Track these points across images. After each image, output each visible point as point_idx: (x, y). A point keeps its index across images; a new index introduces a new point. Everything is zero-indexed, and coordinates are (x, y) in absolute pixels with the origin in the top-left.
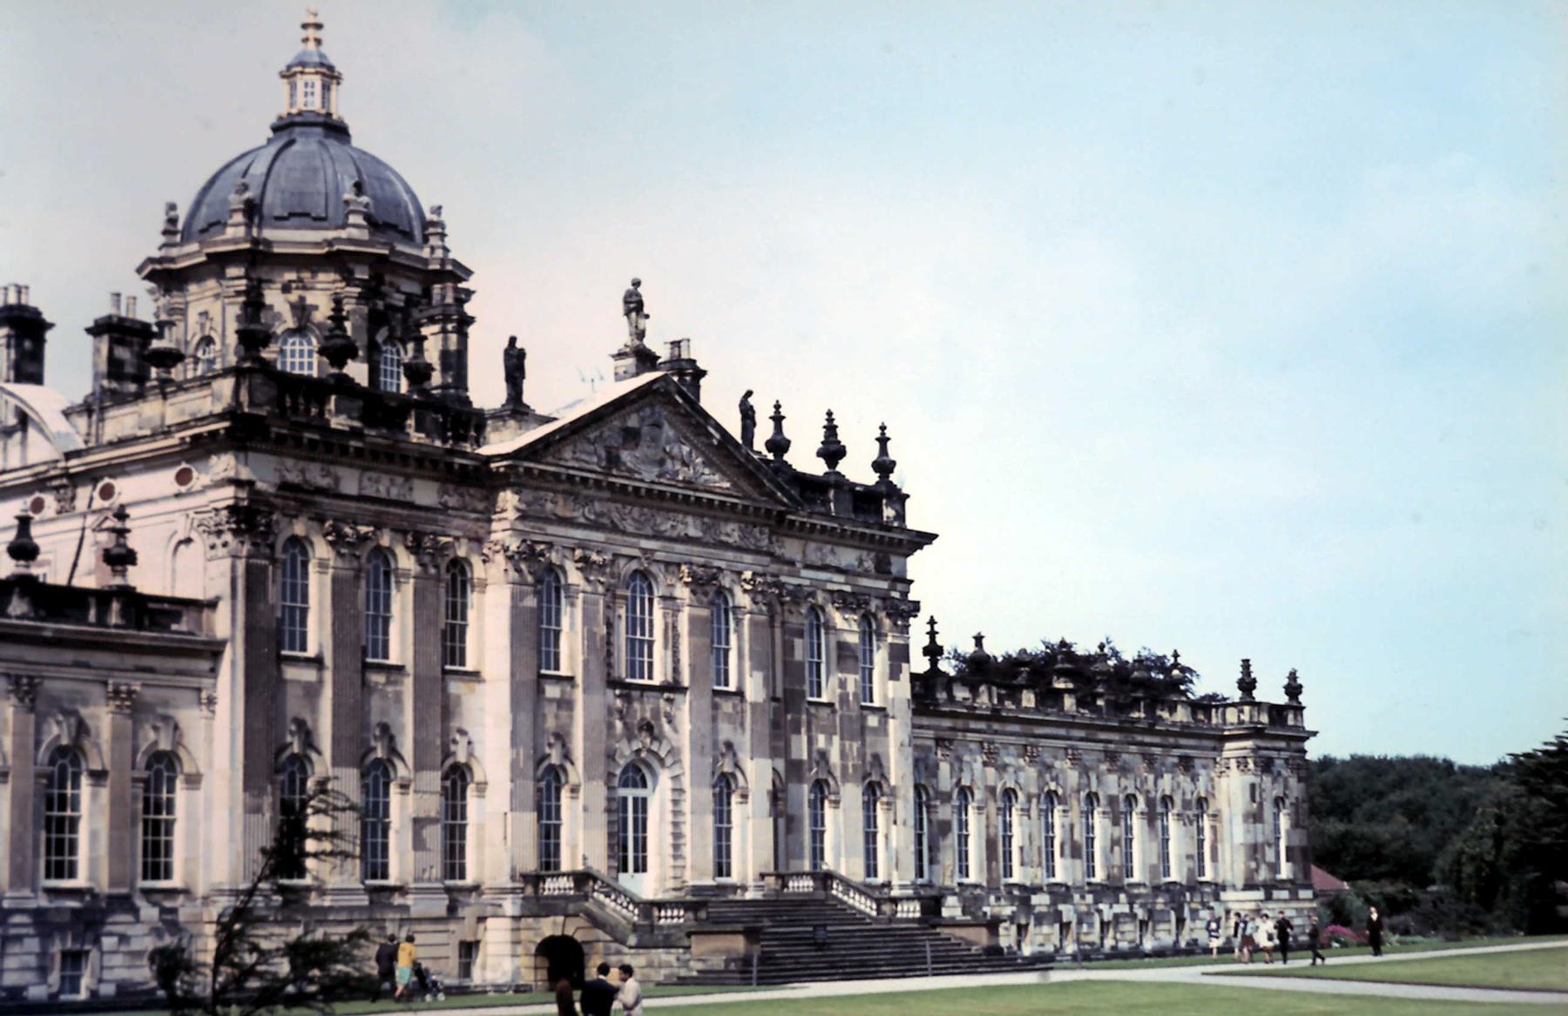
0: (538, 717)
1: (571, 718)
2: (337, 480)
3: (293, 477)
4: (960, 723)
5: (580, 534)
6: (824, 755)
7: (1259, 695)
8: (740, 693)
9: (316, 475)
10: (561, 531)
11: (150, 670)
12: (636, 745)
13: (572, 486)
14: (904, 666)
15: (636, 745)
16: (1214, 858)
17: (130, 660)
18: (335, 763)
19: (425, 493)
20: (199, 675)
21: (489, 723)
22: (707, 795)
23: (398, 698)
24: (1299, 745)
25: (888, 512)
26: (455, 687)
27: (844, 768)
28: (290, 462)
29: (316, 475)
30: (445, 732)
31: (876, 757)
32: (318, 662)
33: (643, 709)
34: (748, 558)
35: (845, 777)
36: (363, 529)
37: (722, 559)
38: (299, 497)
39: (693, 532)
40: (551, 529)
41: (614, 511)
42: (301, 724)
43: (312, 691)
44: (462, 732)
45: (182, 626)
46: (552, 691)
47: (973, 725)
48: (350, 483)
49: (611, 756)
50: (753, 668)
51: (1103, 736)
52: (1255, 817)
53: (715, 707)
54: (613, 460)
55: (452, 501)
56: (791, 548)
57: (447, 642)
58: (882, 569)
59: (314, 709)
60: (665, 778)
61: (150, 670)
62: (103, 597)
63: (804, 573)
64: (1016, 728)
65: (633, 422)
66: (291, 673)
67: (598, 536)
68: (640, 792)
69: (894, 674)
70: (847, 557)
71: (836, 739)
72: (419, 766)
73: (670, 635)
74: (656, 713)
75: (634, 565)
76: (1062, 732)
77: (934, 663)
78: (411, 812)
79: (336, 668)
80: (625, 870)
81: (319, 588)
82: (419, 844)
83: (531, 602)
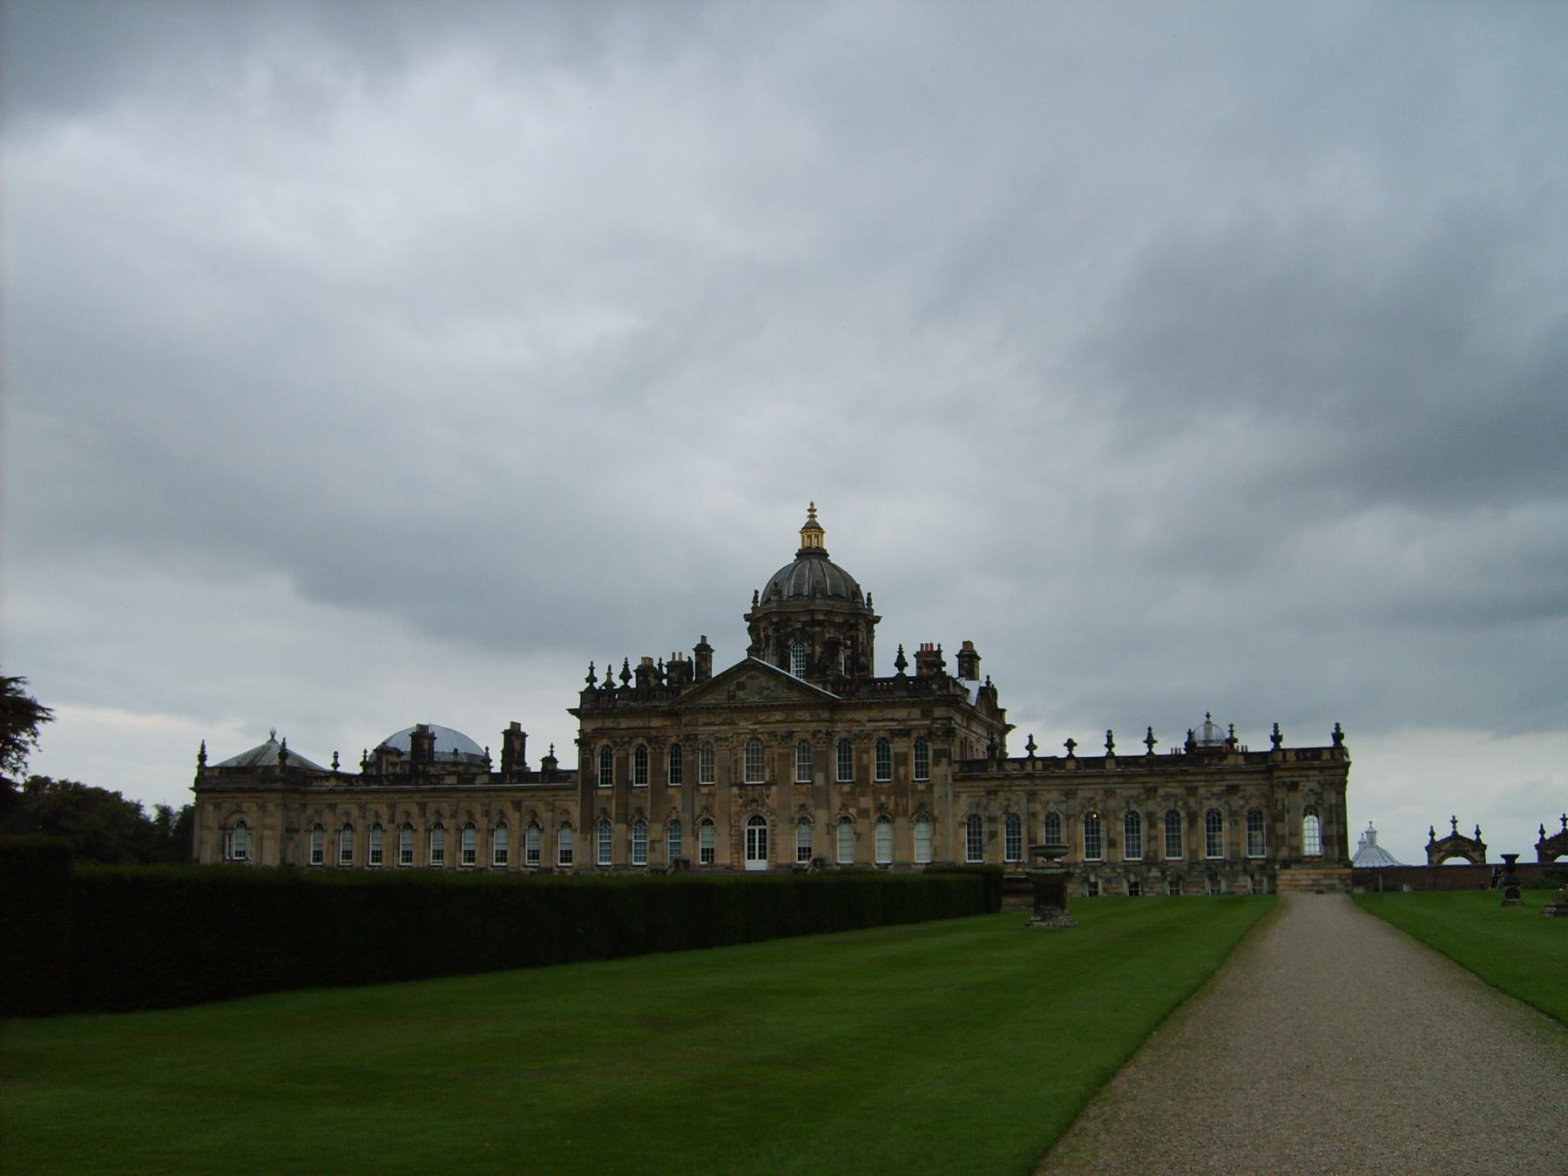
3: (600, 725)
4: (1006, 783)
7: (1283, 745)
9: (609, 724)
13: (710, 710)
14: (944, 760)
26: (670, 791)
29: (609, 724)
35: (897, 814)
38: (601, 732)
48: (624, 724)
54: (732, 697)
56: (861, 715)
58: (926, 714)
64: (1058, 781)
65: (743, 679)
66: (600, 792)
70: (901, 714)
74: (761, 795)
82: (652, 849)
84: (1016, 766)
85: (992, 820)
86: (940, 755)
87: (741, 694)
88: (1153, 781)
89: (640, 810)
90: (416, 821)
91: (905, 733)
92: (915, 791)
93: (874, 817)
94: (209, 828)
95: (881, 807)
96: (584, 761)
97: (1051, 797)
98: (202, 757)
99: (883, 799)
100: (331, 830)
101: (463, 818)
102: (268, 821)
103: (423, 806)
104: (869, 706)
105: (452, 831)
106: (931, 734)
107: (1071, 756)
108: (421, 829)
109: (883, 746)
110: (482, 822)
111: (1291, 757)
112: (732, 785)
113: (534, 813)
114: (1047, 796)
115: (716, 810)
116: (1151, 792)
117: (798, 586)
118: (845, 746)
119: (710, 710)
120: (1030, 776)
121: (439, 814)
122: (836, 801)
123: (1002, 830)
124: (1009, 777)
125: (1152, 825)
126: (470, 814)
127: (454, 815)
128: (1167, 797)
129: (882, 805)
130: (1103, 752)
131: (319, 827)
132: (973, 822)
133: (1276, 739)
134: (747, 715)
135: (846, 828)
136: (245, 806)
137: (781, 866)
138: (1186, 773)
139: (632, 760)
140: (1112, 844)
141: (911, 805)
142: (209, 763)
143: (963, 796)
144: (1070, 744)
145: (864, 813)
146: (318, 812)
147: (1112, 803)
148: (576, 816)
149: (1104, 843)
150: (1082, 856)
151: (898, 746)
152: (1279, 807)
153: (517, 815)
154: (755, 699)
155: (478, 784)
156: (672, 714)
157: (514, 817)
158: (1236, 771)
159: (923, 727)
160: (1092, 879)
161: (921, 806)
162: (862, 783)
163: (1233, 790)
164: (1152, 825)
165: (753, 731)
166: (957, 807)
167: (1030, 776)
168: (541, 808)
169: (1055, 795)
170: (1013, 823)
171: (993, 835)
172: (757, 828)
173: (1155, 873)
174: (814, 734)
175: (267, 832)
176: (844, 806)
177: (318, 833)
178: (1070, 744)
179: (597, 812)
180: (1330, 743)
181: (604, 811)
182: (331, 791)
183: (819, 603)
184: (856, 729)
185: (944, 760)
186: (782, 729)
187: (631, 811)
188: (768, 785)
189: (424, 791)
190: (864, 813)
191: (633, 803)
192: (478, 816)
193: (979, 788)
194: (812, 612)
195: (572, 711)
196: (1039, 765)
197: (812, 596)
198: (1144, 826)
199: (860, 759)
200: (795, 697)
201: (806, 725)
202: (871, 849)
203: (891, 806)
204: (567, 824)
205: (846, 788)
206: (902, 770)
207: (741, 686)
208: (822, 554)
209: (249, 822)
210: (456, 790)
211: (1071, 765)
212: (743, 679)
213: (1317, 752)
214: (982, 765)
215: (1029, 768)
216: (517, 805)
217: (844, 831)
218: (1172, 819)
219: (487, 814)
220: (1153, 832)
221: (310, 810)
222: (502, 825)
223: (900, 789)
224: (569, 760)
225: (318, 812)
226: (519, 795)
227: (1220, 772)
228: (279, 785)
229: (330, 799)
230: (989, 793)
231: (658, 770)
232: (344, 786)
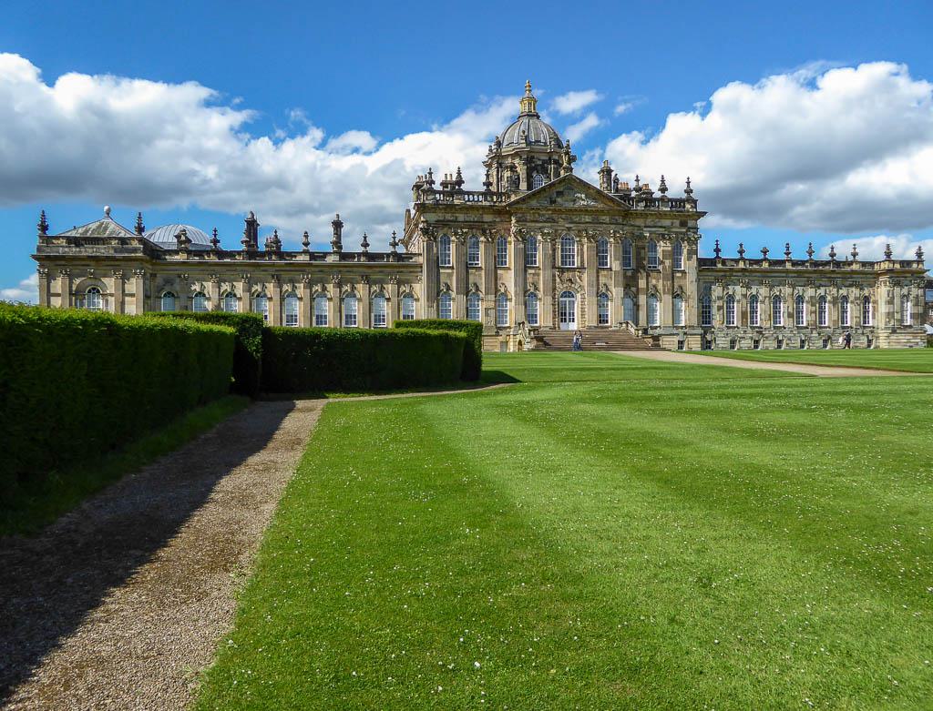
0: (525, 279)
1: (539, 279)
2: (456, 217)
5: (540, 225)
6: (655, 286)
8: (611, 269)
10: (533, 224)
11: (401, 272)
12: (565, 285)
14: (694, 257)
15: (565, 285)
16: (874, 318)
17: (396, 270)
18: (457, 293)
19: (488, 218)
20: (417, 272)
21: (509, 280)
22: (595, 299)
23: (480, 275)
24: (921, 275)
25: (688, 206)
27: (664, 290)
28: (440, 215)
29: (449, 217)
30: (496, 284)
31: (681, 287)
32: (452, 268)
33: (567, 275)
34: (613, 226)
36: (464, 230)
39: (587, 220)
40: (528, 224)
41: (555, 216)
42: (446, 284)
43: (450, 275)
44: (503, 284)
45: (413, 260)
46: (530, 271)
47: (734, 274)
48: (461, 217)
49: (554, 289)
50: (615, 259)
51: (807, 275)
52: (891, 302)
53: (598, 272)
55: (497, 220)
56: (639, 222)
57: (498, 261)
58: (683, 224)
59: (451, 280)
60: (579, 296)
61: (401, 272)
62: (388, 255)
63: (645, 229)
66: (441, 271)
67: (549, 224)
68: (572, 299)
69: (689, 258)
70: (667, 222)
71: (661, 281)
72: (487, 294)
73: (582, 251)
74: (574, 276)
75: (564, 232)
76: (784, 275)
77: (717, 254)
78: (484, 307)
79: (457, 269)
80: (565, 321)
81: (453, 246)
82: (487, 315)
83: (522, 246)
84: (733, 263)
85: (719, 298)
87: (559, 200)
94: (58, 295)
96: (429, 248)
98: (44, 228)
99: (654, 282)
107: (765, 259)
108: (277, 298)
111: (897, 266)
112: (554, 267)
115: (541, 286)
117: (537, 134)
129: (655, 286)
130: (784, 257)
131: (169, 294)
134: (563, 216)
137: (590, 327)
142: (49, 233)
143: (701, 283)
144: (765, 252)
146: (168, 282)
148: (420, 289)
149: (786, 315)
152: (891, 296)
154: (570, 205)
157: (361, 289)
159: (681, 233)
160: (780, 338)
165: (569, 229)
172: (567, 299)
173: (815, 334)
175: (127, 298)
177: (169, 300)
178: (765, 252)
180: (915, 258)
181: (449, 288)
185: (694, 257)
188: (582, 268)
189: (281, 265)
193: (710, 276)
196: (747, 262)
203: (660, 287)
205: (629, 273)
207: (560, 194)
208: (538, 117)
211: (765, 265)
213: (909, 263)
214: (712, 262)
220: (814, 308)
221: (159, 280)
228: (141, 255)
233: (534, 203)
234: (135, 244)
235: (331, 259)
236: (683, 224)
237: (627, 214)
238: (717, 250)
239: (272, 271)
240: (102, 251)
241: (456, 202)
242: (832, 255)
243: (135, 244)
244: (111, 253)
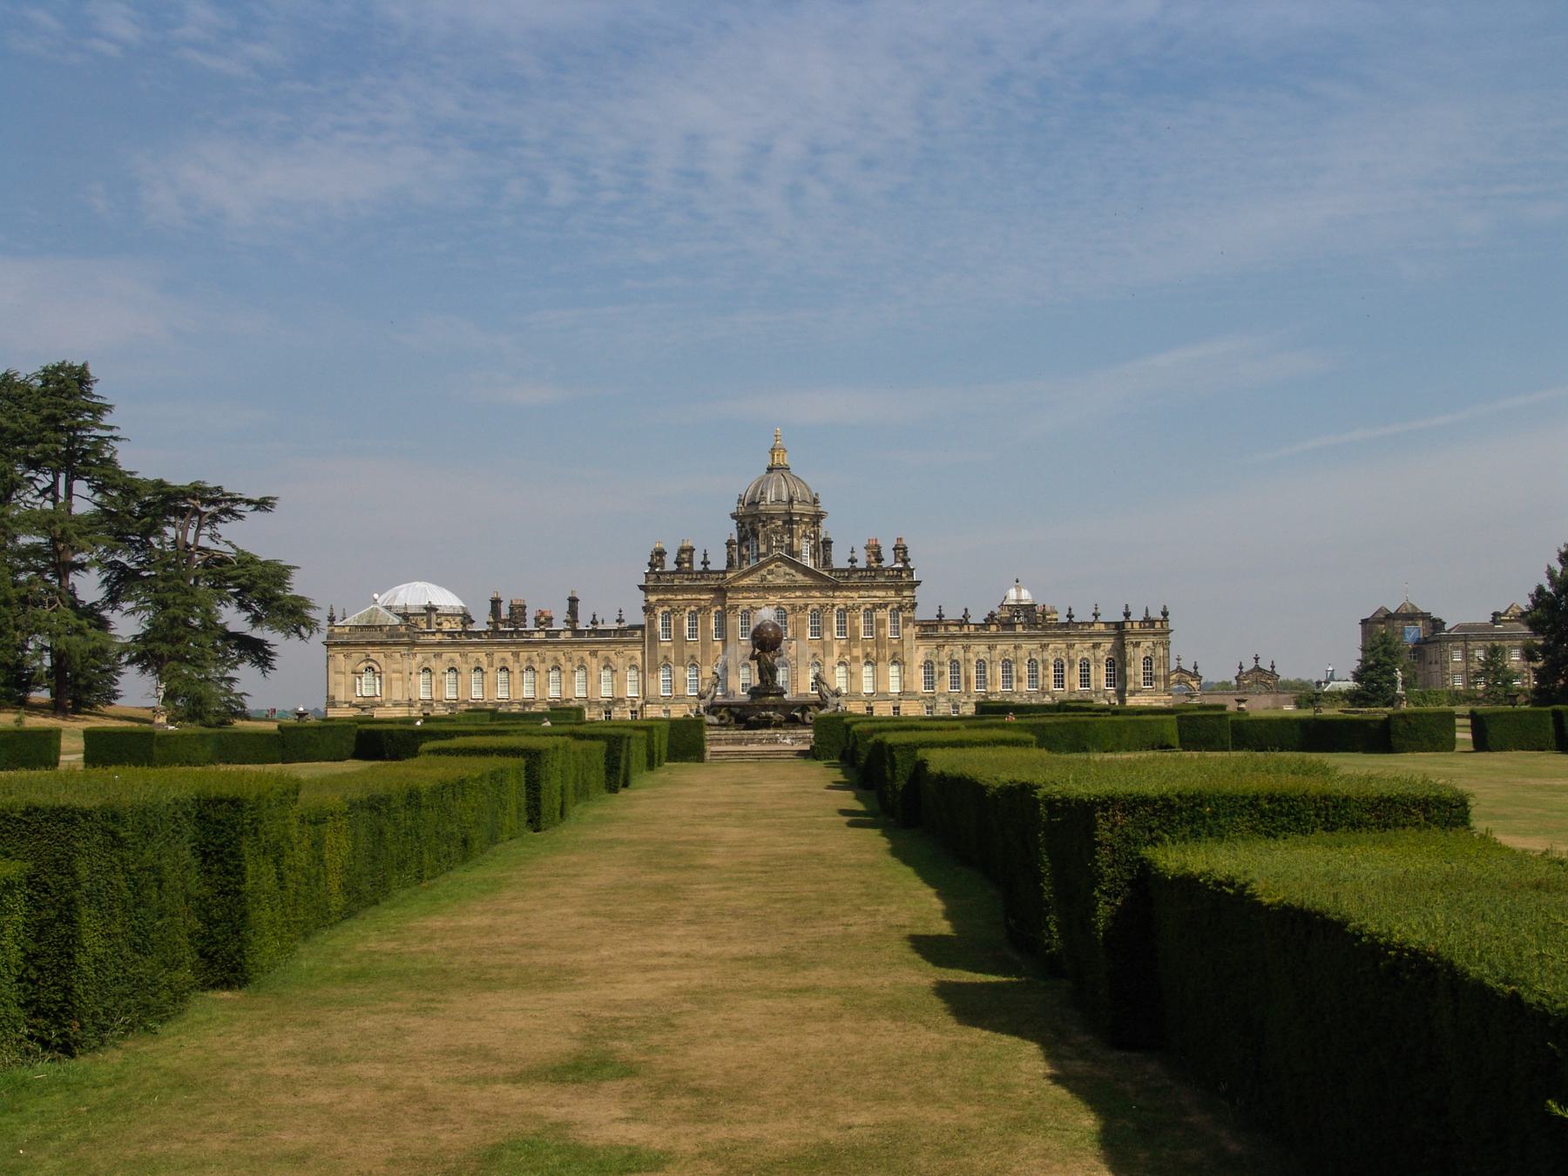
13: (748, 589)
37: (809, 601)
54: (763, 579)
86: (907, 621)
88: (1045, 641)
89: (692, 657)
90: (510, 664)
91: (886, 606)
92: (891, 645)
93: (863, 662)
95: (867, 655)
97: (980, 649)
100: (439, 673)
101: (550, 664)
102: (395, 666)
103: (516, 655)
104: (857, 588)
105: (543, 672)
106: (900, 608)
108: (517, 671)
109: (869, 613)
110: (567, 666)
111: (1136, 625)
113: (607, 659)
114: (977, 648)
116: (1044, 647)
117: (778, 494)
118: (842, 613)
119: (748, 589)
120: (967, 636)
121: (529, 659)
122: (836, 651)
123: (947, 670)
124: (954, 637)
125: (1045, 668)
126: (556, 659)
127: (543, 661)
128: (1055, 650)
131: (426, 670)
132: (928, 666)
133: (1127, 615)
135: (842, 669)
136: (373, 656)
138: (1067, 635)
139: (686, 621)
140: (1020, 680)
141: (888, 654)
145: (856, 659)
147: (1021, 653)
150: (999, 688)
151: (882, 614)
153: (595, 661)
154: (780, 581)
155: (562, 637)
156: (721, 592)
157: (593, 663)
158: (1100, 635)
161: (895, 654)
162: (853, 639)
163: (1096, 646)
164: (1045, 668)
166: (919, 653)
167: (967, 636)
168: (612, 655)
169: (983, 648)
170: (955, 665)
171: (941, 674)
174: (822, 606)
176: (841, 654)
179: (660, 659)
182: (440, 644)
183: (797, 508)
184: (850, 603)
186: (801, 602)
187: (687, 658)
190: (856, 659)
191: (688, 652)
192: (563, 661)
193: (933, 643)
194: (791, 515)
195: (641, 587)
197: (791, 501)
198: (1040, 668)
199: (852, 623)
200: (808, 581)
201: (817, 599)
202: (860, 682)
204: (632, 667)
206: (882, 631)
207: (771, 572)
209: (377, 669)
210: (546, 643)
212: (772, 567)
215: (965, 630)
216: (594, 654)
217: (840, 671)
218: (1059, 667)
219: (570, 660)
222: (581, 667)
223: (879, 643)
224: (636, 617)
225: (425, 659)
226: (596, 647)
227: (1090, 635)
229: (437, 650)
230: (938, 647)
231: (706, 629)
232: (448, 639)
233: (746, 582)
234: (403, 629)
235: (562, 637)
236: (897, 595)
237: (837, 587)
238: (940, 616)
239: (513, 649)
240: (379, 637)
241: (676, 582)
242: (1070, 616)
243: (403, 629)
244: (384, 638)
